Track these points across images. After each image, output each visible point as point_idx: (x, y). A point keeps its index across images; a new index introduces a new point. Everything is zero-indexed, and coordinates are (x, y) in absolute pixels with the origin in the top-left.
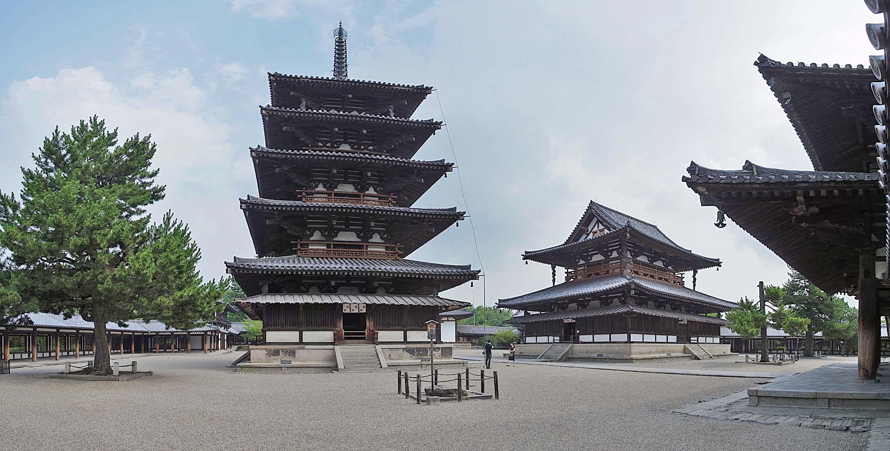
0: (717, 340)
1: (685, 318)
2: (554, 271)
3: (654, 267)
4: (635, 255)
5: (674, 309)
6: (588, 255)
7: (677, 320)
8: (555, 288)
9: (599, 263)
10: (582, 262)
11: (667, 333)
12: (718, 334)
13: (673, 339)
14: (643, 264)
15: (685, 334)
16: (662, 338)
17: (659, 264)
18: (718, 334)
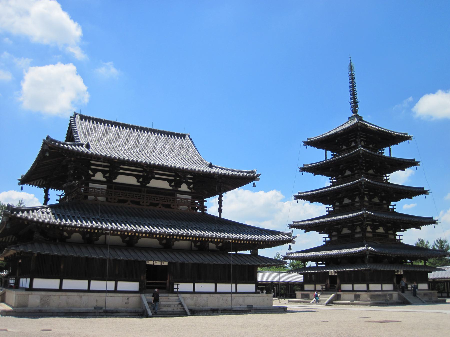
0: (251, 287)
12: (252, 279)
18: (252, 279)
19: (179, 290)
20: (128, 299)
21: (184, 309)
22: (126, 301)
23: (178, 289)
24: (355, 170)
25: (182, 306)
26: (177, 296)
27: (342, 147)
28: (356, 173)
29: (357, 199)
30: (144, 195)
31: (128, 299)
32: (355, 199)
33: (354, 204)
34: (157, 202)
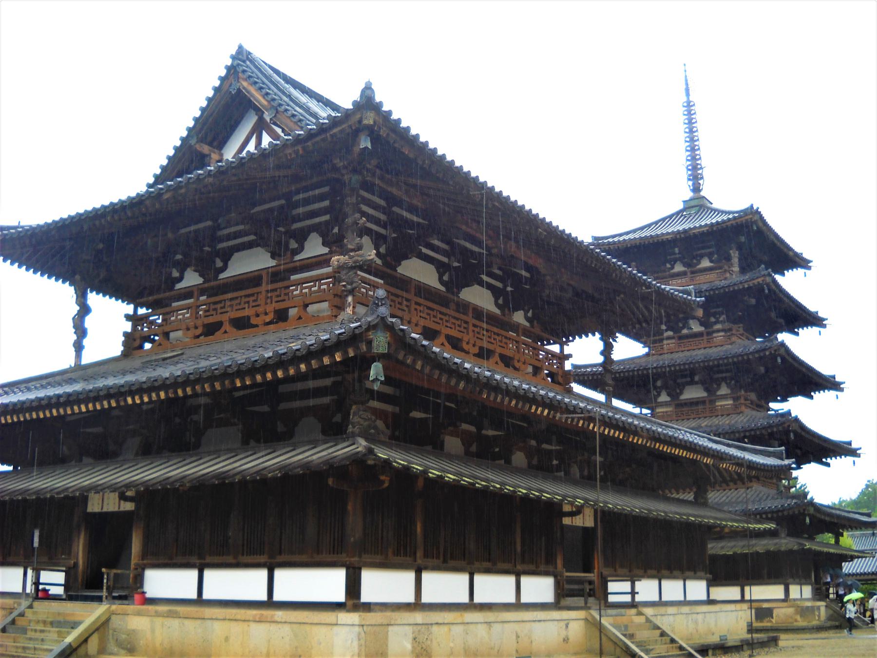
1: (583, 503)
2: (84, 310)
3: (463, 307)
4: (395, 254)
5: (541, 467)
6: (217, 253)
7: (553, 510)
8: (79, 371)
9: (252, 280)
10: (192, 279)
11: (518, 565)
13: (539, 588)
14: (423, 291)
15: (582, 562)
16: (494, 587)
17: (478, 296)
19: (638, 598)
20: (567, 626)
21: (681, 648)
22: (564, 633)
23: (633, 593)
24: (715, 323)
25: (673, 641)
26: (640, 614)
27: (673, 268)
28: (718, 331)
29: (724, 390)
30: (466, 322)
31: (567, 626)
32: (719, 387)
33: (712, 402)
34: (491, 347)
